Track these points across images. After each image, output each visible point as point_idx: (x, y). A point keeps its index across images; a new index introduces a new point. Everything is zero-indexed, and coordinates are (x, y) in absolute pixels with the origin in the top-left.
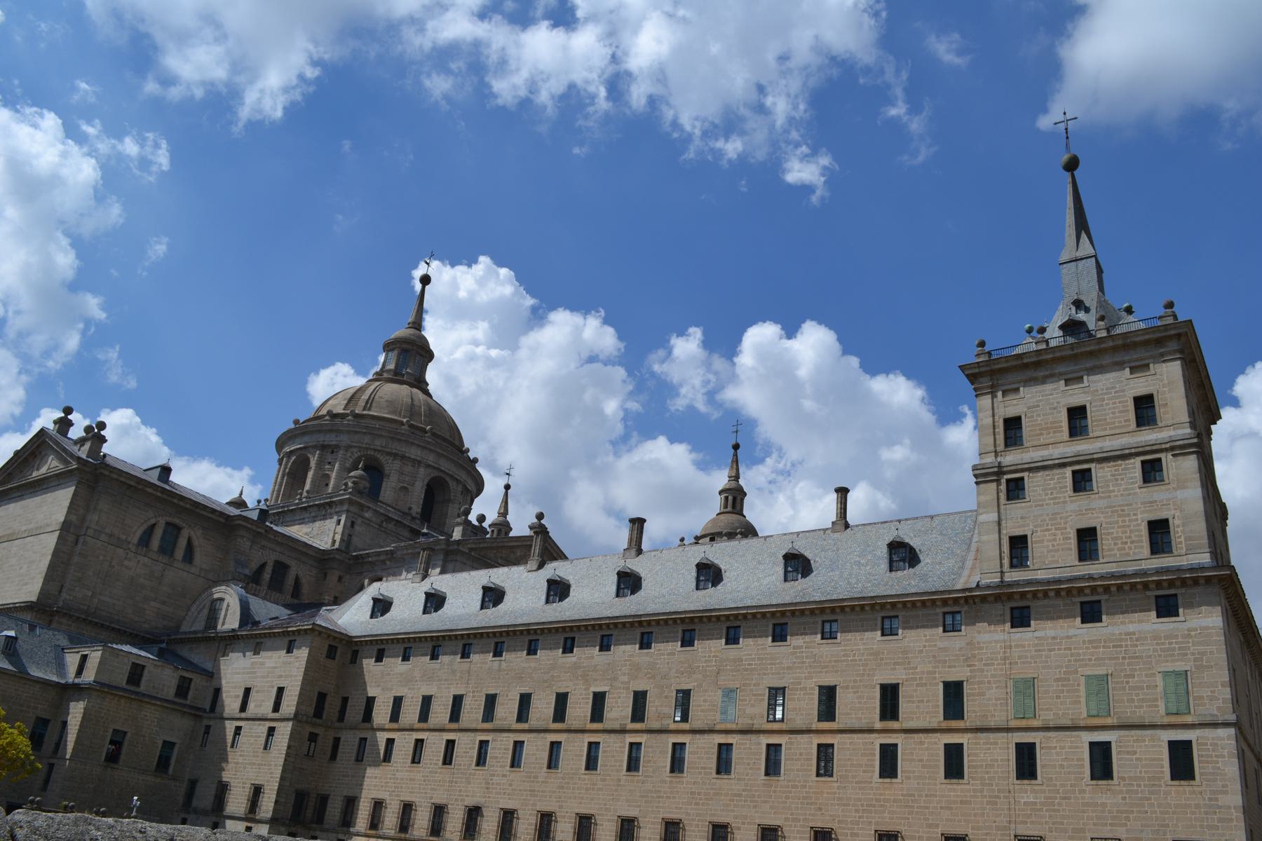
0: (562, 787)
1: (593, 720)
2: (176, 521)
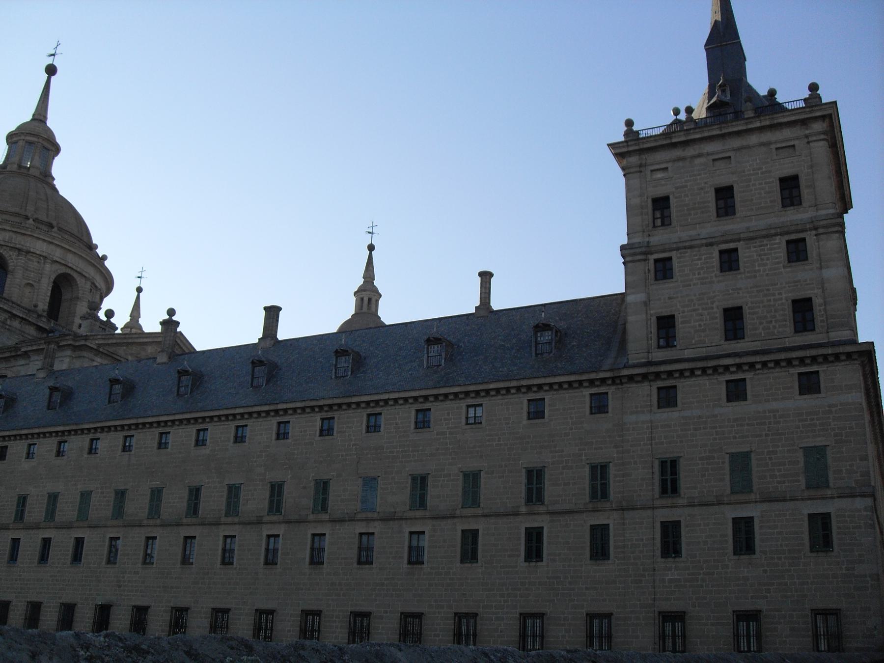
1: (227, 515)
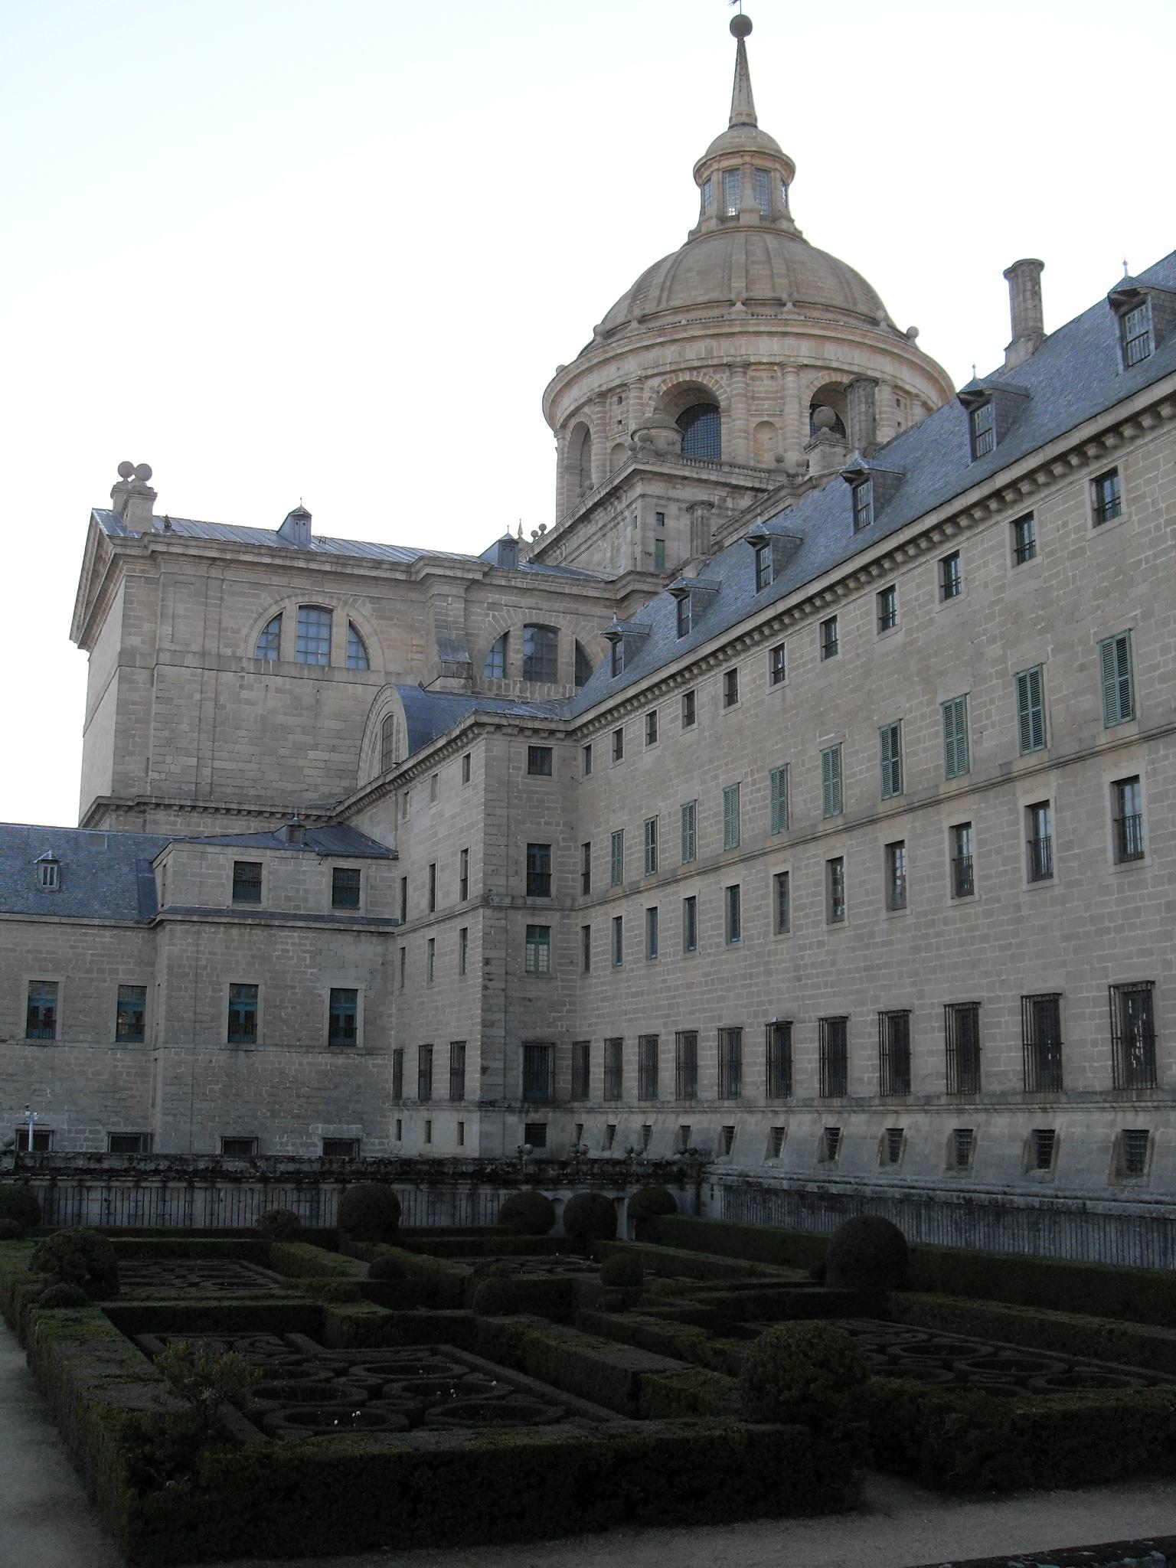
0: (917, 949)
2: (318, 600)
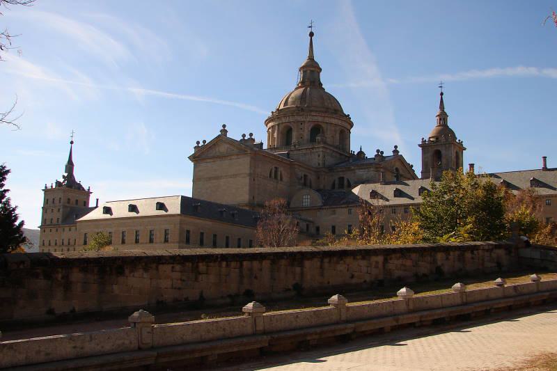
2: (277, 166)
